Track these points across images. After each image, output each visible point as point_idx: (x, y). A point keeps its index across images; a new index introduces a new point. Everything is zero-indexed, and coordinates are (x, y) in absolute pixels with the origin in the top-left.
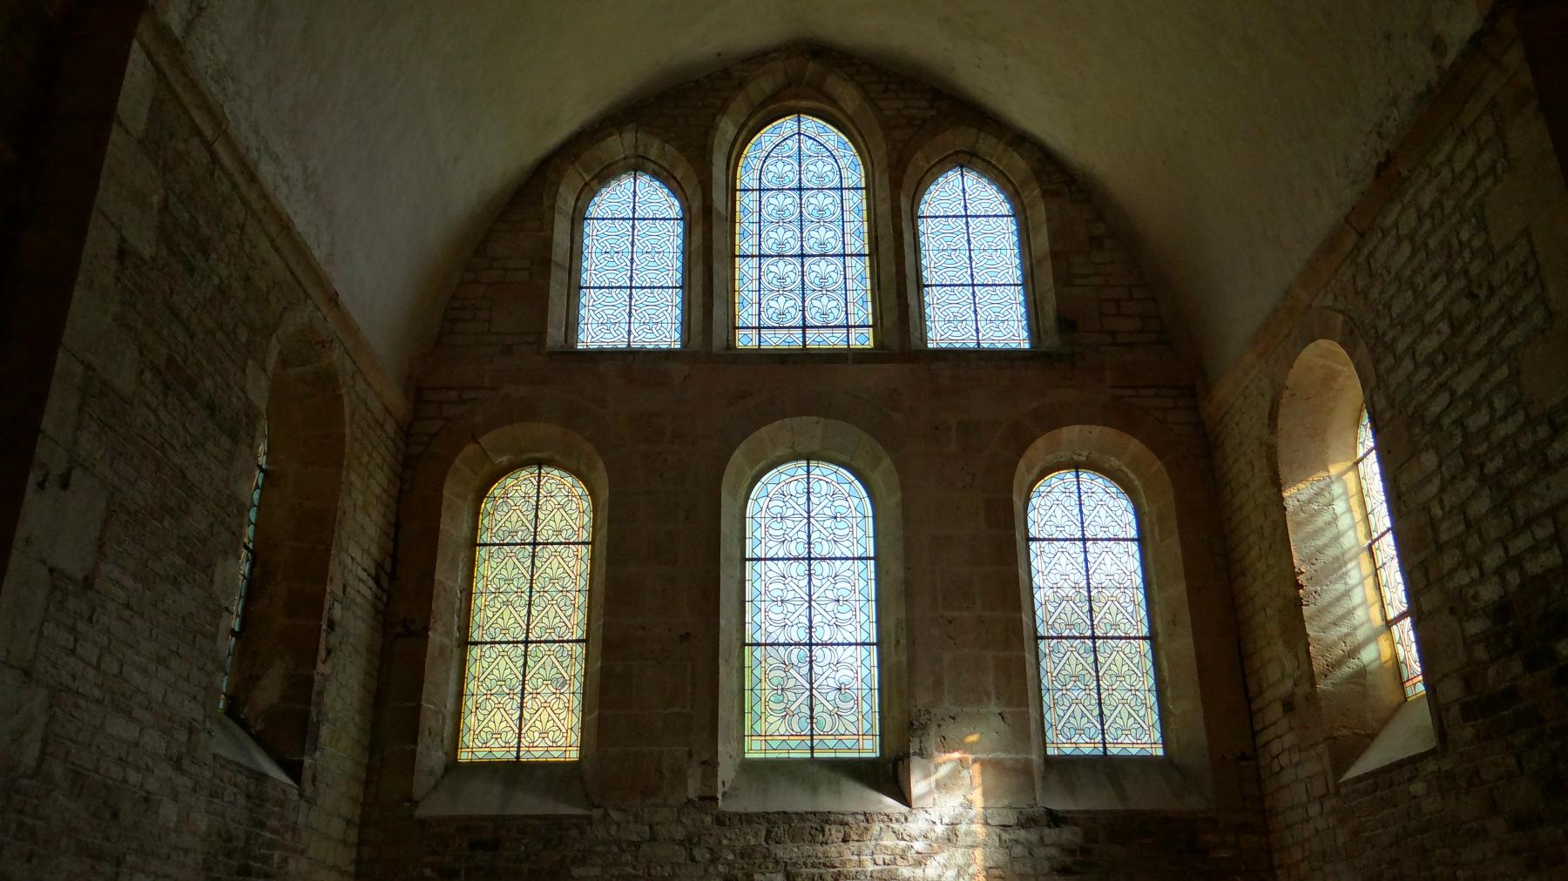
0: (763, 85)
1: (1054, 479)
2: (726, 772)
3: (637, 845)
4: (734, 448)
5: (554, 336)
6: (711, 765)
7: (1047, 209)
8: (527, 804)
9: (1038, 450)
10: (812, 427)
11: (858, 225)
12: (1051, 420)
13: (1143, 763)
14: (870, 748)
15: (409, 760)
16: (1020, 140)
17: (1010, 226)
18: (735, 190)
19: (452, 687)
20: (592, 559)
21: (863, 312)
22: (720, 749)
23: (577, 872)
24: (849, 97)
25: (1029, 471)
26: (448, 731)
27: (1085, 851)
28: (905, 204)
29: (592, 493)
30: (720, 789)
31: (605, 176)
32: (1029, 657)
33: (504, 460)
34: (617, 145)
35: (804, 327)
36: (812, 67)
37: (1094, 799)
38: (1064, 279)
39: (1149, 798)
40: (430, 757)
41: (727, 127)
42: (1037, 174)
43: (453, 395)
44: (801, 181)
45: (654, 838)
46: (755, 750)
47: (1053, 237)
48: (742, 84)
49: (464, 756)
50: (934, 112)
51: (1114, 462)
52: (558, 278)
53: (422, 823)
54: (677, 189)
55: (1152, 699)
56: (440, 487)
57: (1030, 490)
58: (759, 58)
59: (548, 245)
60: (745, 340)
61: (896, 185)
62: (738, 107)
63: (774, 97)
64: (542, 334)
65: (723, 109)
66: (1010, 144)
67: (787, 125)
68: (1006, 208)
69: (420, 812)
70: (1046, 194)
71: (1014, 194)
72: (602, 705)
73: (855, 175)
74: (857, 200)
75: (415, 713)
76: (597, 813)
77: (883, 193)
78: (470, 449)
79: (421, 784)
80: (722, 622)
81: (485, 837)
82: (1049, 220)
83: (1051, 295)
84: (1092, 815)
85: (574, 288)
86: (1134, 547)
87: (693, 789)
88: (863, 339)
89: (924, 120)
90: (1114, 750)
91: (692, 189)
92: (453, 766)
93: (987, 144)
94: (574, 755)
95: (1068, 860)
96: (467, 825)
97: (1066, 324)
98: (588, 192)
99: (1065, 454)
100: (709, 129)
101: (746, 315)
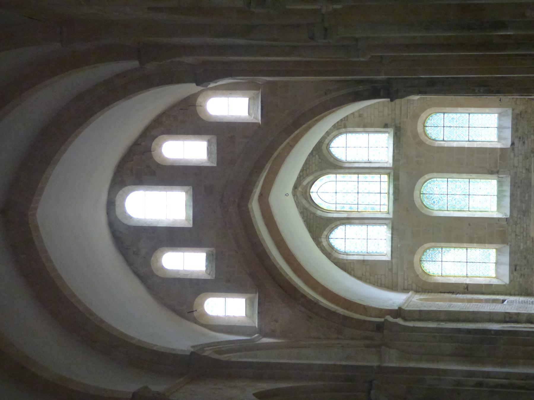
0: (304, 202)
1: (428, 132)
2: (500, 216)
3: (516, 235)
4: (422, 213)
5: (388, 258)
6: (499, 219)
7: (350, 127)
8: (506, 259)
9: (423, 137)
10: (416, 193)
11: (348, 177)
12: (416, 135)
13: (499, 119)
15: (497, 286)
16: (328, 133)
17: (349, 135)
18: (336, 211)
19: (478, 279)
20: (446, 247)
21: (376, 177)
22: (495, 216)
23: (522, 248)
24: (310, 178)
25: (427, 141)
26: (489, 279)
27: (520, 138)
28: (347, 165)
29: (429, 248)
30: (504, 217)
31: (332, 248)
32: (475, 145)
33: (420, 269)
34: (325, 244)
35: (380, 193)
36: (300, 189)
38: (372, 126)
39: (508, 122)
40: (495, 282)
41: (319, 213)
42: (338, 129)
43: (406, 282)
45: (515, 232)
46: (494, 208)
47: (359, 127)
48: (306, 209)
49: (494, 275)
50: (317, 156)
51: (424, 118)
52: (367, 258)
53: (511, 281)
54: (336, 226)
55: (484, 115)
56: (430, 283)
57: (430, 139)
58: (298, 204)
59: (358, 261)
60: (385, 209)
61: (341, 168)
62: (312, 209)
63: (306, 199)
64: (385, 261)
65: (314, 214)
66: (328, 136)
67: (314, 196)
68: (344, 136)
69: (508, 282)
70: (345, 127)
71: (341, 134)
72: (485, 243)
73: (332, 177)
74: (340, 177)
75: (486, 285)
76: (509, 243)
77: (342, 171)
78: (420, 276)
79: (500, 283)
80: (466, 216)
81: (514, 268)
82: (353, 127)
83: (376, 129)
84: (512, 136)
85: (368, 254)
86: (446, 115)
87: (505, 223)
88: (385, 178)
89: (319, 158)
90: (496, 126)
91: (338, 222)
92: (496, 277)
93: (327, 141)
94: (494, 250)
95: (521, 142)
96: (511, 272)
97: (386, 126)
98: (336, 251)
99: (422, 130)
100: (321, 218)
101: (377, 208)
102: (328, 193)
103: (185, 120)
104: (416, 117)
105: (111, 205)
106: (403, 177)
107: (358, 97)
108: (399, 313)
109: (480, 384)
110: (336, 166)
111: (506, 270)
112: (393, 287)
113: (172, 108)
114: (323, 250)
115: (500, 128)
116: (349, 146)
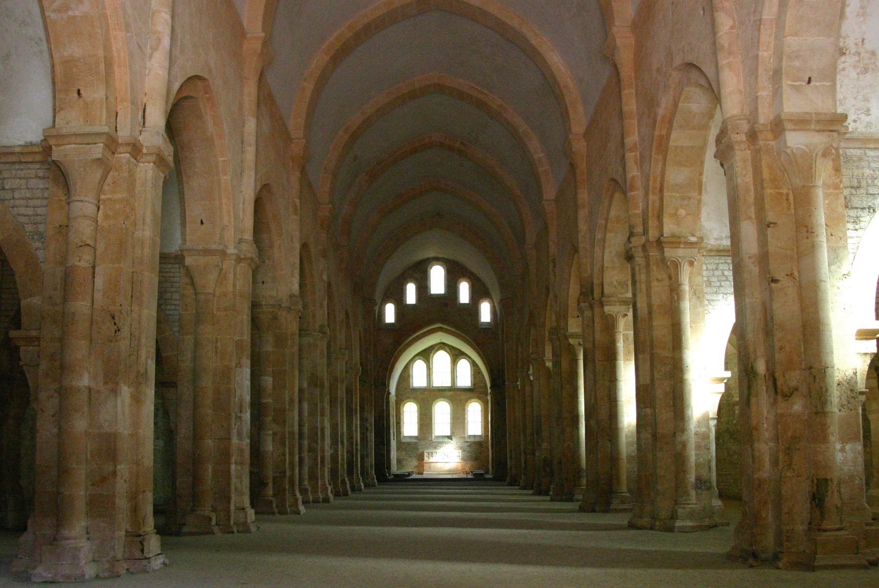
14: (449, 434)
16: (470, 358)
37: (472, 440)
39: (477, 440)
44: (441, 358)
81: (409, 444)
88: (450, 385)
102: (441, 358)
103: (478, 294)
104: (479, 398)
105: (437, 260)
106: (451, 393)
107: (491, 371)
108: (389, 393)
109: (367, 429)
110: (454, 362)
111: (408, 440)
112: (397, 389)
113: (484, 285)
114: (414, 357)
115: (475, 436)
116: (464, 369)
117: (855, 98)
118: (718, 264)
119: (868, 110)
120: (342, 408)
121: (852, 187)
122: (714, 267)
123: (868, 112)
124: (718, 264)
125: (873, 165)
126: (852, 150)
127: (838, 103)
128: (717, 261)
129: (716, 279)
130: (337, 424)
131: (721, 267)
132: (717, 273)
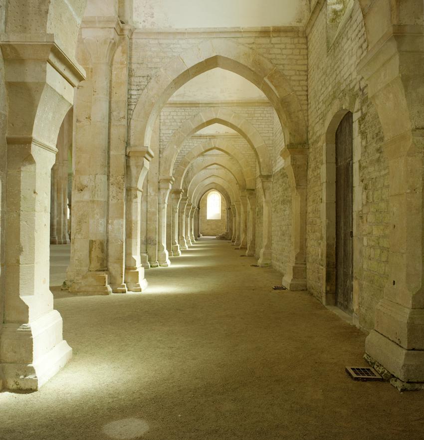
117: (145, 7)
118: (170, 112)
119: (153, 14)
120: (64, 194)
121: (138, 63)
122: (168, 114)
123: (152, 16)
124: (170, 112)
125: (153, 49)
126: (140, 40)
127: (134, 10)
128: (170, 110)
129: (168, 121)
130: (61, 204)
131: (172, 114)
132: (169, 117)
